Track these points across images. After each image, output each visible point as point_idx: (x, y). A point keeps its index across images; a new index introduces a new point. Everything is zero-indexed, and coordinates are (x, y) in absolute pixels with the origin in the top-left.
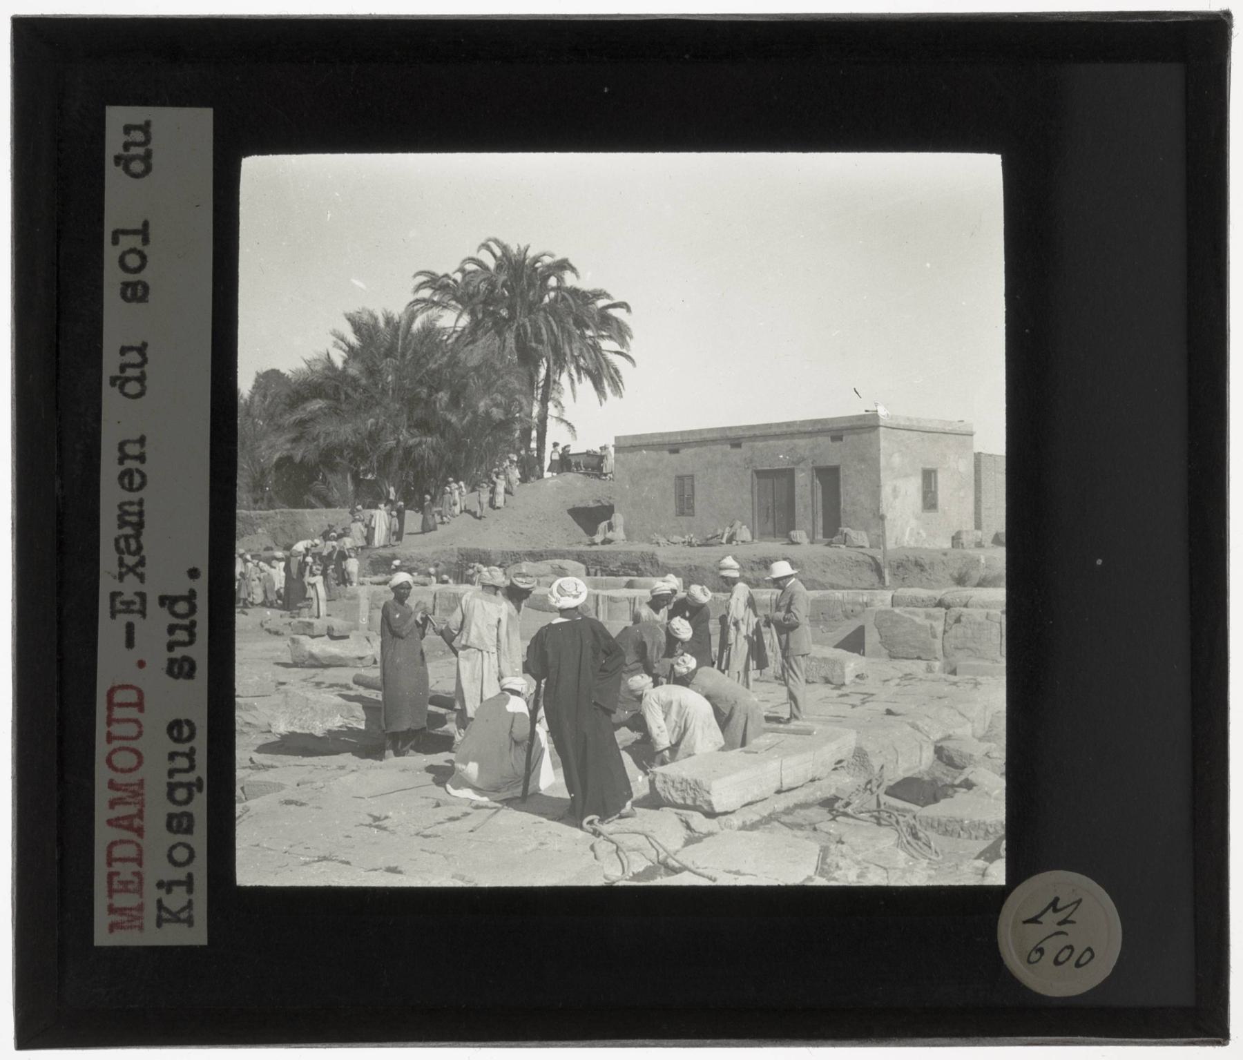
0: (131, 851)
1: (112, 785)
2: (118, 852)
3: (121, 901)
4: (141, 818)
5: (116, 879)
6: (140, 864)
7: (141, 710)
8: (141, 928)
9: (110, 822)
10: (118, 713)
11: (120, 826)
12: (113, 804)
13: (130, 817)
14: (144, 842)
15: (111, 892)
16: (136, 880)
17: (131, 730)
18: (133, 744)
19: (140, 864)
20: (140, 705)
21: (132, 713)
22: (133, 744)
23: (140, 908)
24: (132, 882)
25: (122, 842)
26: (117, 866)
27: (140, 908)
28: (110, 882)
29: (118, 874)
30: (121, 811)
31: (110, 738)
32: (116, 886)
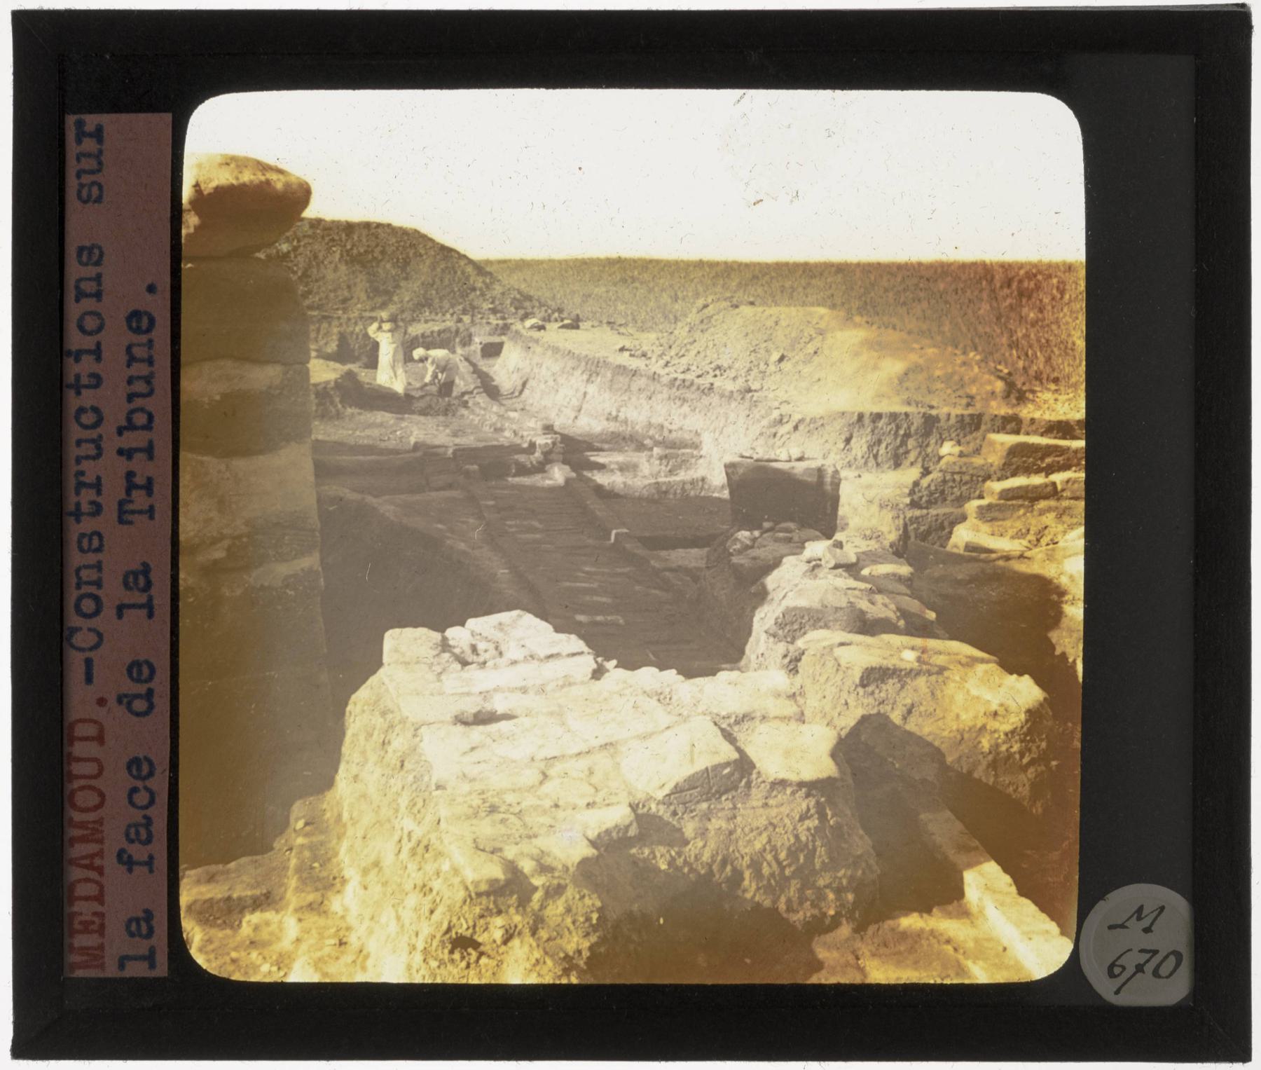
0: (91, 890)
3: (81, 941)
4: (102, 858)
5: (76, 922)
6: (102, 903)
8: (102, 967)
13: (92, 856)
16: (96, 919)
18: (93, 782)
19: (102, 903)
22: (93, 782)
24: (93, 923)
25: (87, 880)
27: (101, 947)
29: (81, 914)
32: (77, 926)
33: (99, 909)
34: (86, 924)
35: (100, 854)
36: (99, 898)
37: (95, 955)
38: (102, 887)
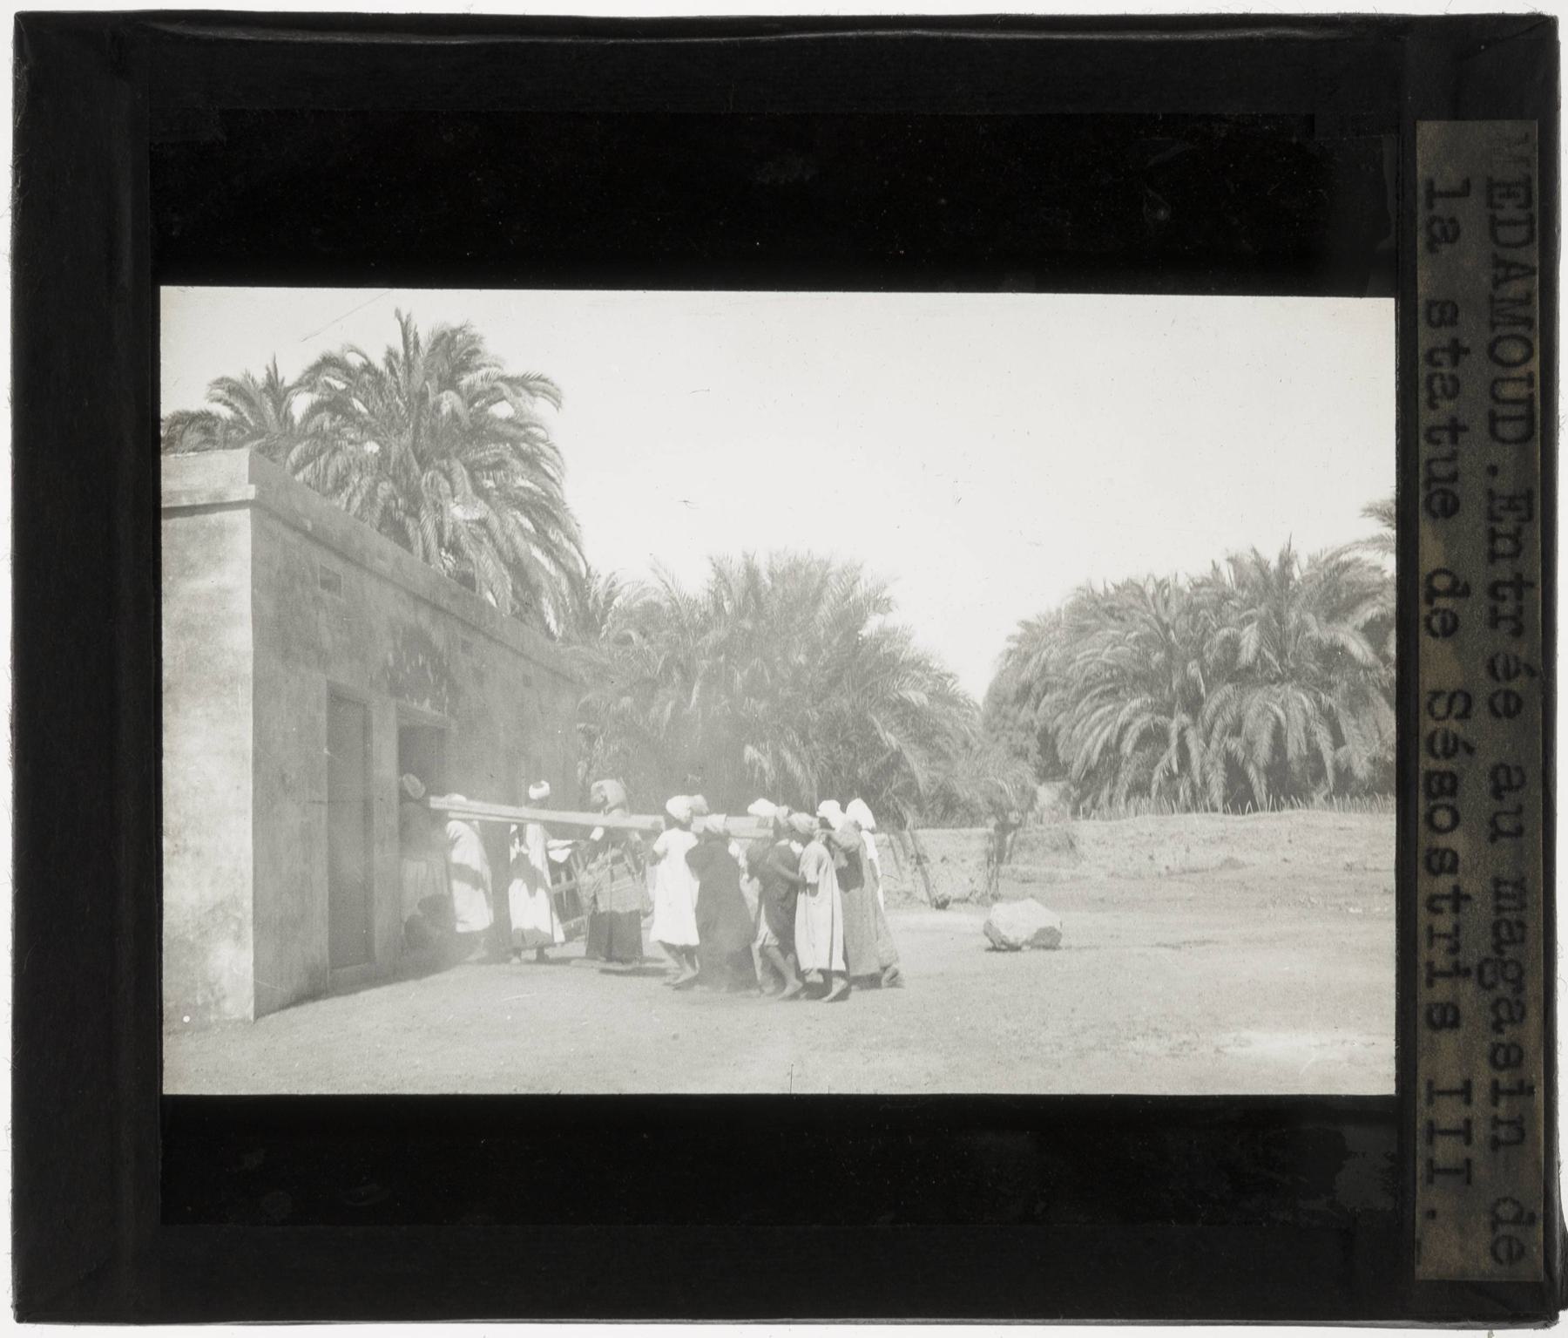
0: (1505, 234)
2: (1520, 233)
6: (1493, 218)
13: (1507, 279)
16: (1497, 200)
19: (1493, 218)
24: (1501, 196)
29: (1519, 207)
32: (1521, 191)
34: (1509, 195)
35: (1497, 283)
36: (1494, 223)
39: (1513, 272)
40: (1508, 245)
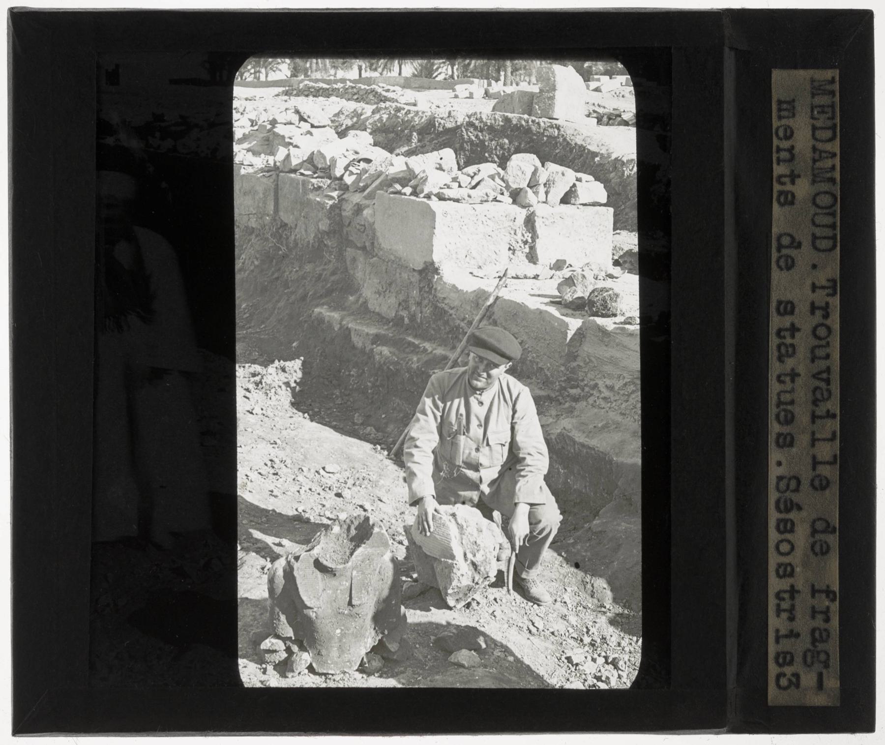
0: (819, 134)
1: (832, 180)
2: (828, 134)
5: (830, 115)
7: (814, 235)
9: (834, 155)
10: (828, 232)
11: (826, 152)
12: (833, 168)
13: (821, 158)
14: (812, 142)
15: (832, 106)
17: (818, 220)
18: (819, 211)
20: (815, 237)
21: (818, 232)
23: (813, 95)
26: (829, 123)
28: (834, 112)
29: (829, 118)
30: (828, 163)
31: (833, 214)
32: (830, 110)
33: (815, 122)
34: (823, 112)
35: (814, 161)
36: (814, 128)
37: (817, 89)
38: (813, 135)
39: (824, 155)
40: (821, 141)
